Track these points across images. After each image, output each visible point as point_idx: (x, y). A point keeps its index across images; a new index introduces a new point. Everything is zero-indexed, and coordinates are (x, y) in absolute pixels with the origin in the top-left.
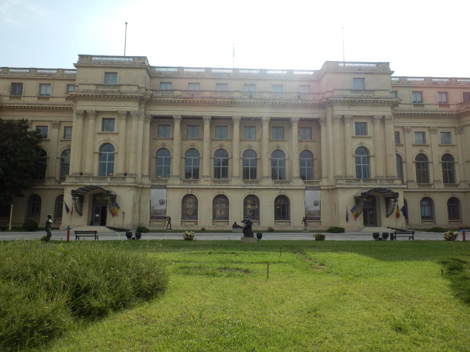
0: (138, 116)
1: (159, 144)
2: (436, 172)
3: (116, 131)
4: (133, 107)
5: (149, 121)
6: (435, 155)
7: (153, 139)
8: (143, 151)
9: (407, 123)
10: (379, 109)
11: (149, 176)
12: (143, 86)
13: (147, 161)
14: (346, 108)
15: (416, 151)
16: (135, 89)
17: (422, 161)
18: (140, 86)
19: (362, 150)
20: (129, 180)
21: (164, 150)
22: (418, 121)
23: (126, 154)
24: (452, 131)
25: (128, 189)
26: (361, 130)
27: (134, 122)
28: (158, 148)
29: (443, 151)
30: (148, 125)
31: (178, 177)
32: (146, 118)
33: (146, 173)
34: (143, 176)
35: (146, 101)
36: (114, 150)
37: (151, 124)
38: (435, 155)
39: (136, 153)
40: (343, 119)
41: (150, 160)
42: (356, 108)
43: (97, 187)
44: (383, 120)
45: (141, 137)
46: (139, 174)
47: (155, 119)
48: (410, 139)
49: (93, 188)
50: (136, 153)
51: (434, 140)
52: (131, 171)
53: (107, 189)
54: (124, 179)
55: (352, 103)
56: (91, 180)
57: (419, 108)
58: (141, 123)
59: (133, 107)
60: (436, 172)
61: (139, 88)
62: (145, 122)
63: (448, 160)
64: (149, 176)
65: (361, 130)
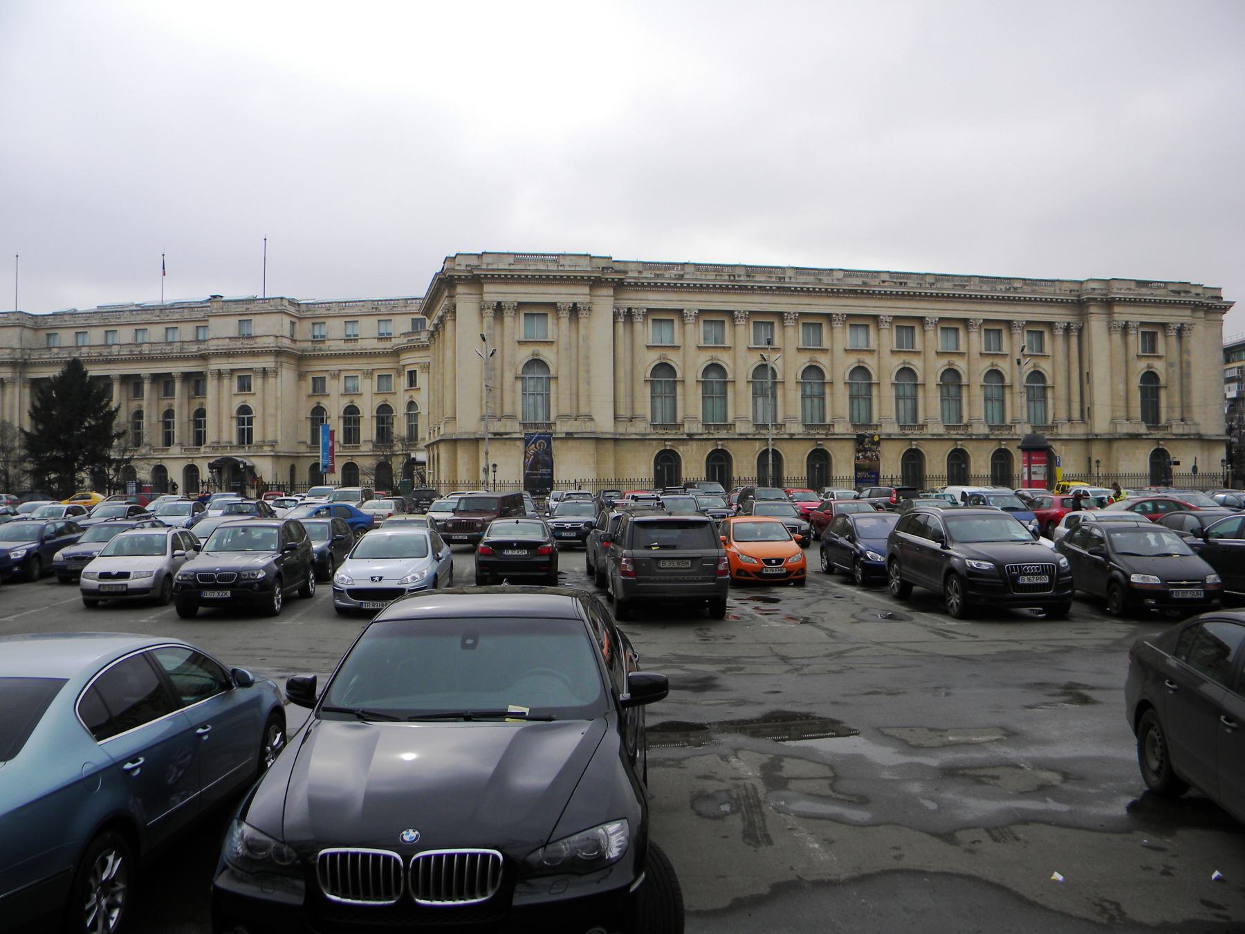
0: (13, 382)
2: (368, 430)
5: (28, 385)
6: (367, 409)
9: (334, 366)
10: (261, 359)
14: (224, 361)
15: (345, 402)
16: (8, 351)
17: (351, 414)
19: (244, 410)
22: (349, 361)
24: (393, 373)
26: (245, 386)
29: (378, 401)
30: (27, 391)
35: (20, 365)
38: (367, 409)
40: (220, 374)
42: (235, 360)
44: (265, 372)
48: (334, 387)
51: (367, 386)
55: (229, 354)
57: (350, 345)
58: (17, 390)
60: (368, 430)
61: (14, 349)
63: (384, 414)
65: (245, 386)
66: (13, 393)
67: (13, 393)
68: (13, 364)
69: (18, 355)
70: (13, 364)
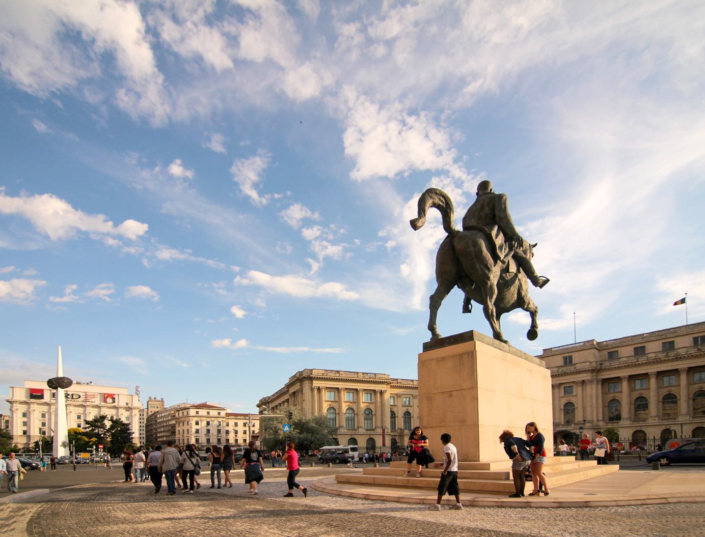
0: (591, 382)
1: (610, 397)
3: (574, 394)
4: (586, 377)
5: (600, 383)
7: (604, 394)
8: (597, 404)
11: (603, 420)
12: (593, 360)
13: (601, 410)
16: (588, 364)
18: (591, 361)
20: (588, 425)
21: (615, 402)
23: (584, 408)
25: (588, 430)
27: (588, 387)
28: (609, 400)
30: (600, 386)
31: (627, 419)
32: (597, 382)
33: (601, 418)
34: (598, 421)
35: (596, 371)
36: (574, 406)
37: (602, 385)
39: (592, 406)
41: (603, 409)
43: (566, 431)
45: (594, 395)
46: (595, 419)
47: (605, 381)
49: (563, 431)
50: (592, 406)
52: (589, 418)
53: (572, 431)
54: (584, 424)
56: (561, 426)
58: (594, 386)
59: (586, 377)
61: (591, 362)
62: (597, 384)
64: (603, 420)
66: (592, 389)
67: (592, 389)
68: (593, 371)
69: (594, 365)
70: (593, 371)
